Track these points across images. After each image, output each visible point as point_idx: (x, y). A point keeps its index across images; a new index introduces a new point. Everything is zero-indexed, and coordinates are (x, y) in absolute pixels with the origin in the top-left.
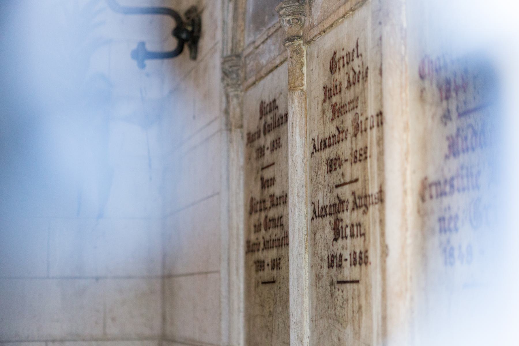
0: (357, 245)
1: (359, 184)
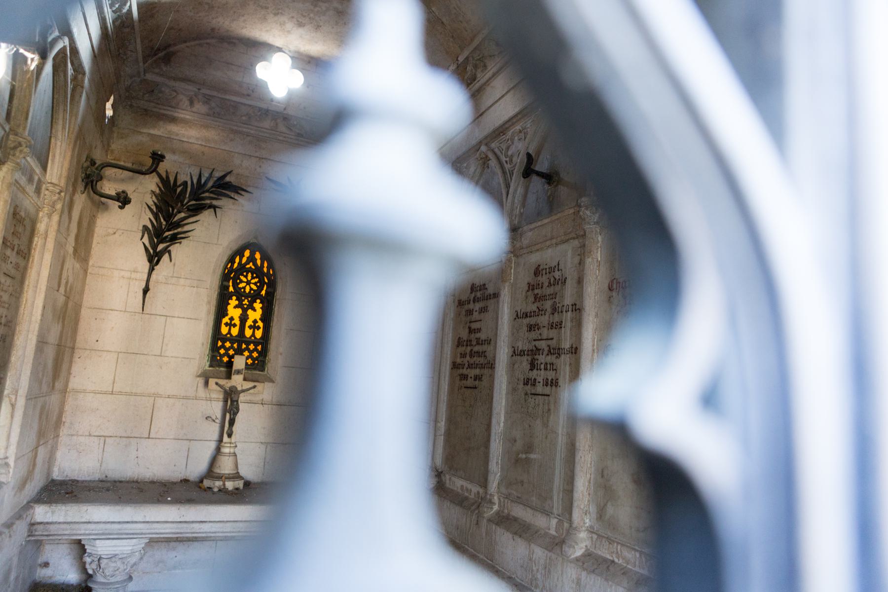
0: (551, 375)
1: (554, 341)
